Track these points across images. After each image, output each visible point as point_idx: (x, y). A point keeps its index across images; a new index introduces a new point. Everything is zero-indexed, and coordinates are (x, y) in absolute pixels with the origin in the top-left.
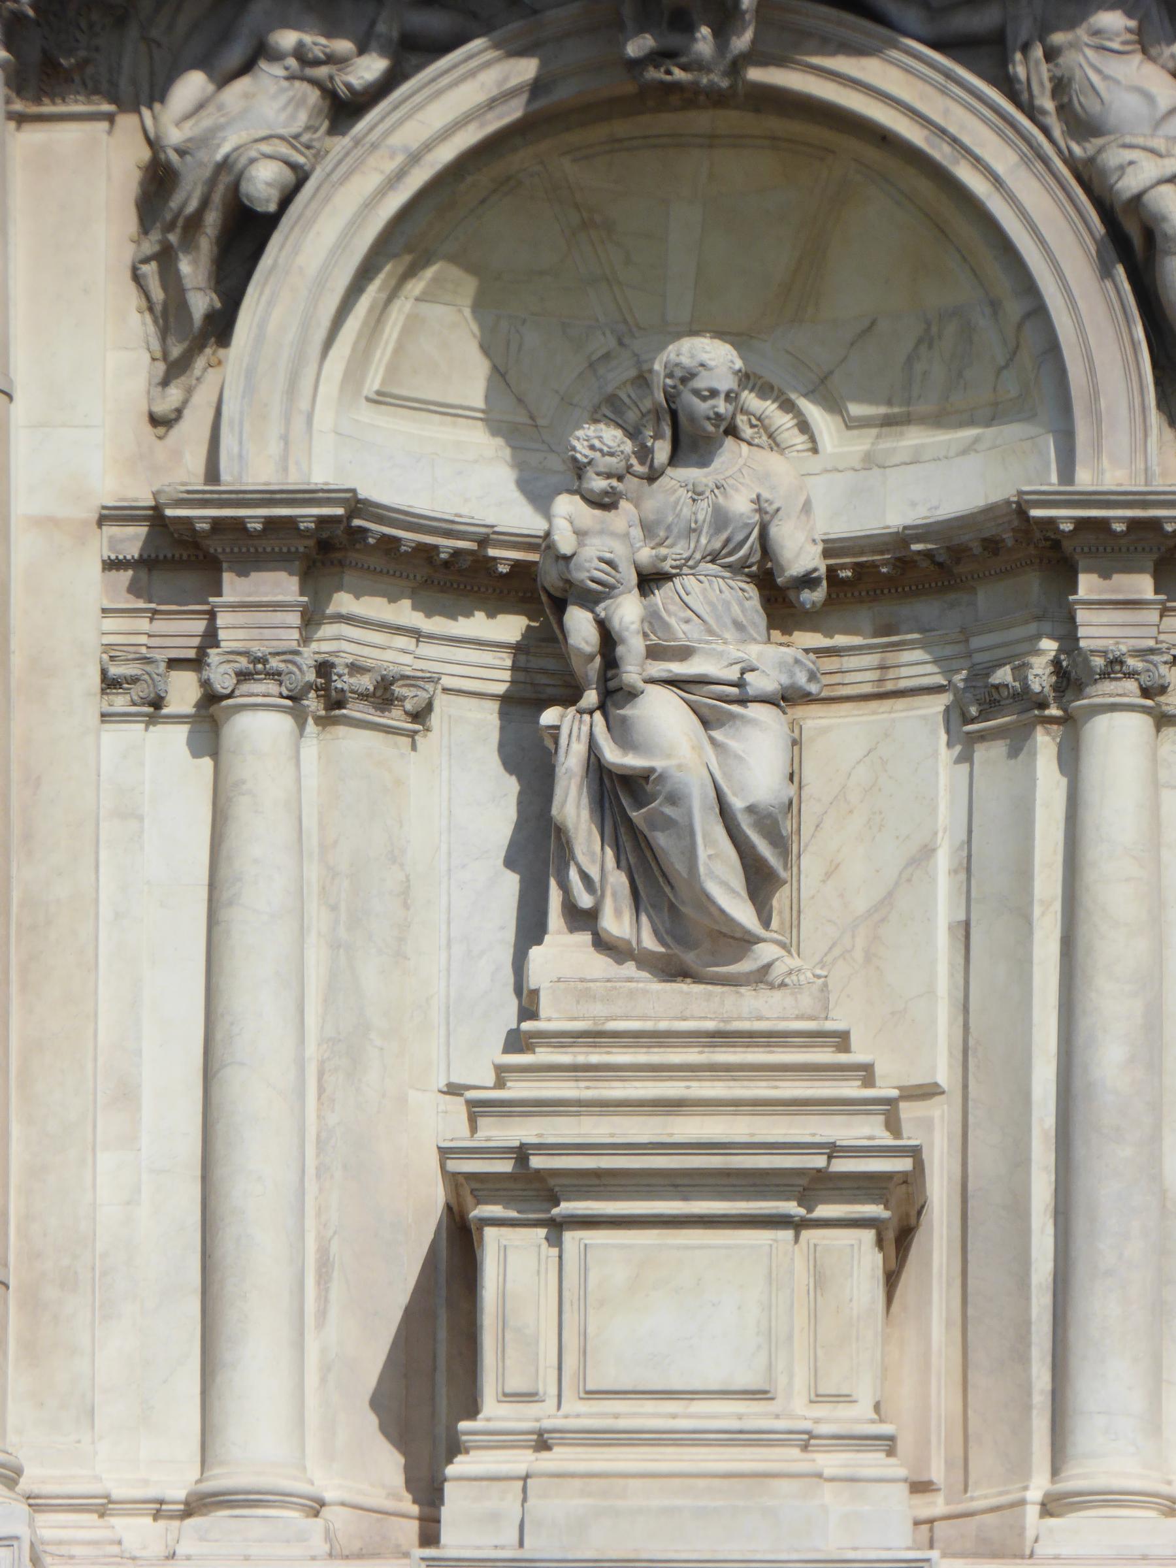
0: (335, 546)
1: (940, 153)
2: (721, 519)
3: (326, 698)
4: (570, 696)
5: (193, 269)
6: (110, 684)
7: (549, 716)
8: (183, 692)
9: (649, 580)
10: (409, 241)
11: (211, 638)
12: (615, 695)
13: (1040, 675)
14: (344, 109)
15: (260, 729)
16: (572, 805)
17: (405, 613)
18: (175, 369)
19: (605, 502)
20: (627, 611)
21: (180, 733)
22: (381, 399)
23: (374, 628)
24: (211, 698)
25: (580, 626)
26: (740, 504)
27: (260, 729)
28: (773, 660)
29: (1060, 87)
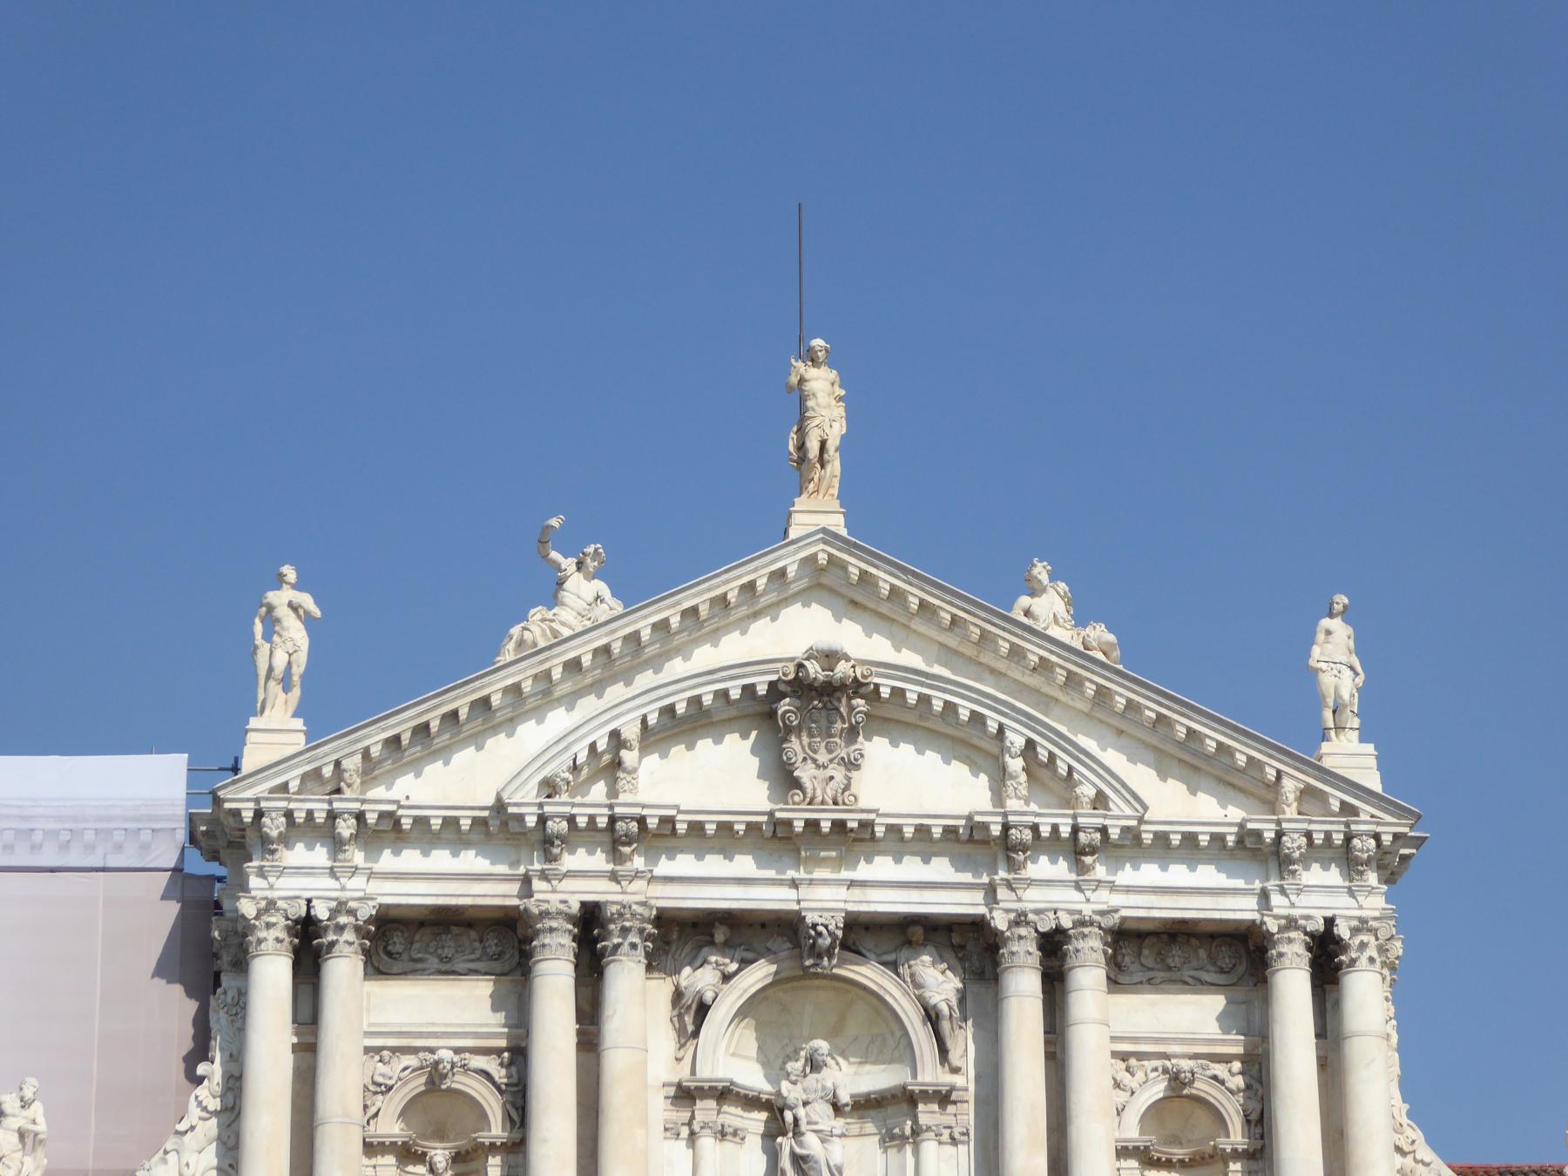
0: (724, 1094)
1: (881, 992)
2: (824, 1088)
3: (722, 1134)
4: (784, 1134)
5: (689, 1019)
6: (666, 1129)
7: (779, 1139)
8: (685, 1132)
9: (805, 1104)
10: (742, 1013)
11: (693, 1117)
12: (797, 1133)
13: (908, 1131)
14: (726, 978)
15: (707, 1142)
16: (786, 1163)
17: (739, 1111)
18: (682, 1046)
19: (794, 1083)
20: (801, 1112)
21: (683, 1143)
22: (733, 1055)
23: (733, 1115)
24: (692, 1133)
25: (788, 1116)
26: (829, 1085)
27: (707, 1142)
28: (839, 1124)
29: (912, 976)
